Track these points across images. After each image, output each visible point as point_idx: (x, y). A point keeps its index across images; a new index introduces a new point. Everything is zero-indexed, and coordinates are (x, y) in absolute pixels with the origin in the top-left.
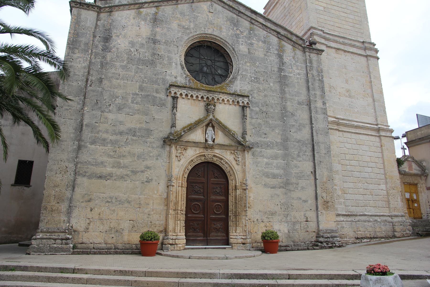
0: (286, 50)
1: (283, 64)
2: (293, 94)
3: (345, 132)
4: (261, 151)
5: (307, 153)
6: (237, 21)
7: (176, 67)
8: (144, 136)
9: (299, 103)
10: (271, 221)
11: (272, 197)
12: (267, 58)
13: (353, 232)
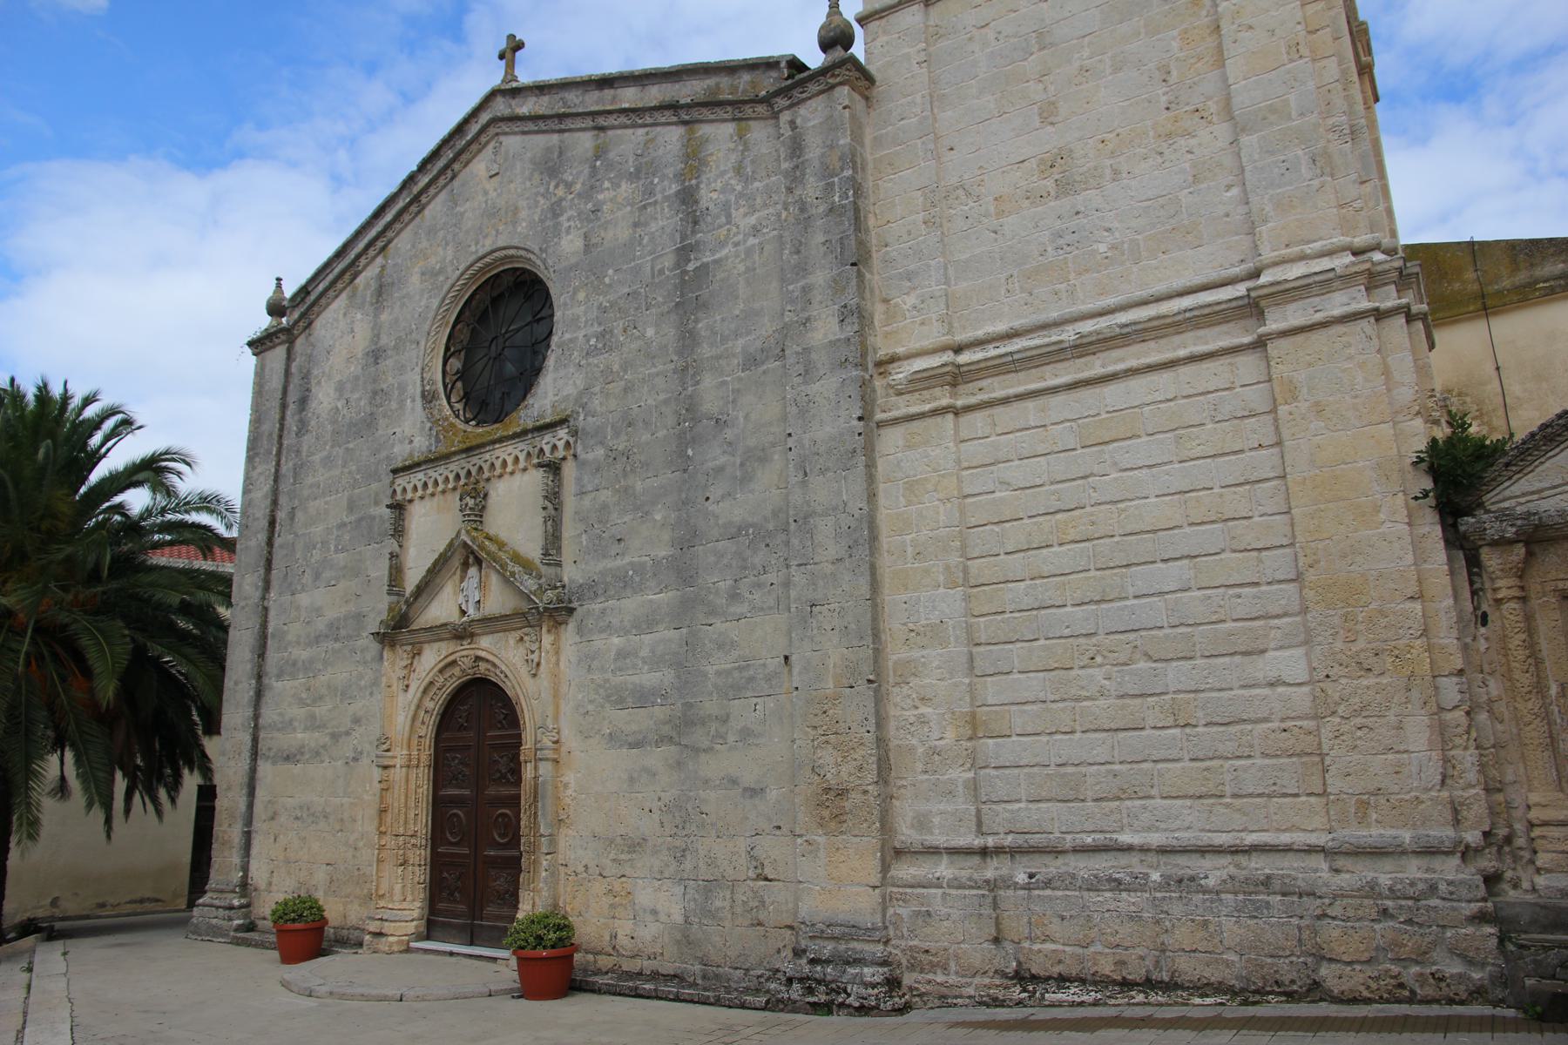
0: (712, 154)
1: (696, 223)
2: (727, 332)
3: (1005, 401)
4: (603, 612)
5: (771, 577)
6: (561, 154)
7: (413, 409)
8: (351, 637)
9: (751, 362)
10: (627, 873)
11: (632, 780)
12: (642, 233)
13: (985, 945)
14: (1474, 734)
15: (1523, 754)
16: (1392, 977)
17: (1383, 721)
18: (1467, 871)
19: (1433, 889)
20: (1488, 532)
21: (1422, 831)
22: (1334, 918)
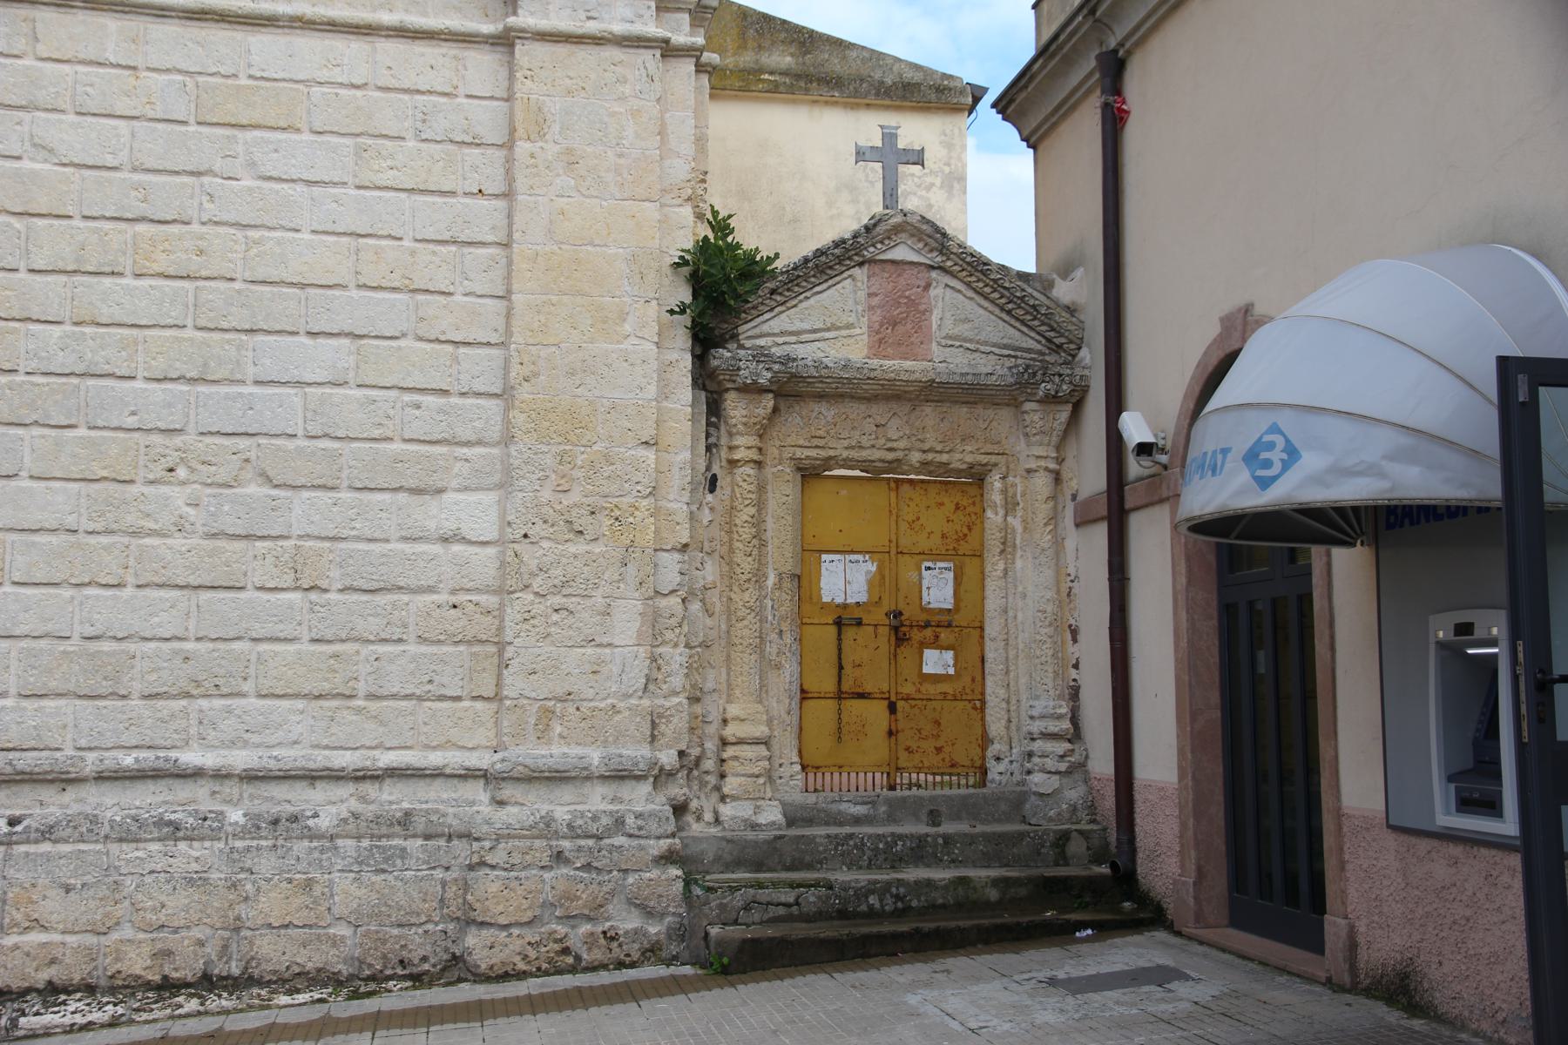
14: (685, 628)
15: (728, 656)
16: (556, 941)
17: (588, 602)
18: (657, 800)
19: (619, 822)
20: (741, 373)
21: (613, 750)
22: (493, 867)
